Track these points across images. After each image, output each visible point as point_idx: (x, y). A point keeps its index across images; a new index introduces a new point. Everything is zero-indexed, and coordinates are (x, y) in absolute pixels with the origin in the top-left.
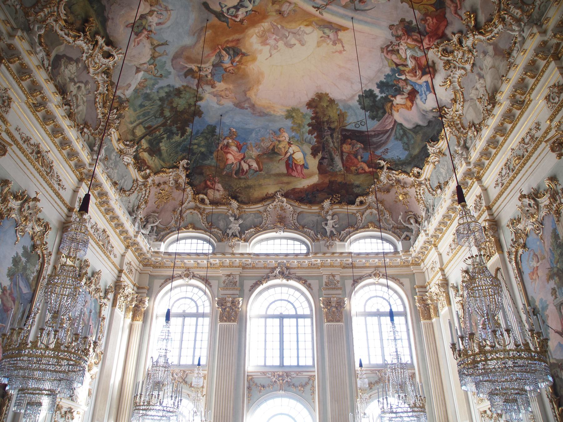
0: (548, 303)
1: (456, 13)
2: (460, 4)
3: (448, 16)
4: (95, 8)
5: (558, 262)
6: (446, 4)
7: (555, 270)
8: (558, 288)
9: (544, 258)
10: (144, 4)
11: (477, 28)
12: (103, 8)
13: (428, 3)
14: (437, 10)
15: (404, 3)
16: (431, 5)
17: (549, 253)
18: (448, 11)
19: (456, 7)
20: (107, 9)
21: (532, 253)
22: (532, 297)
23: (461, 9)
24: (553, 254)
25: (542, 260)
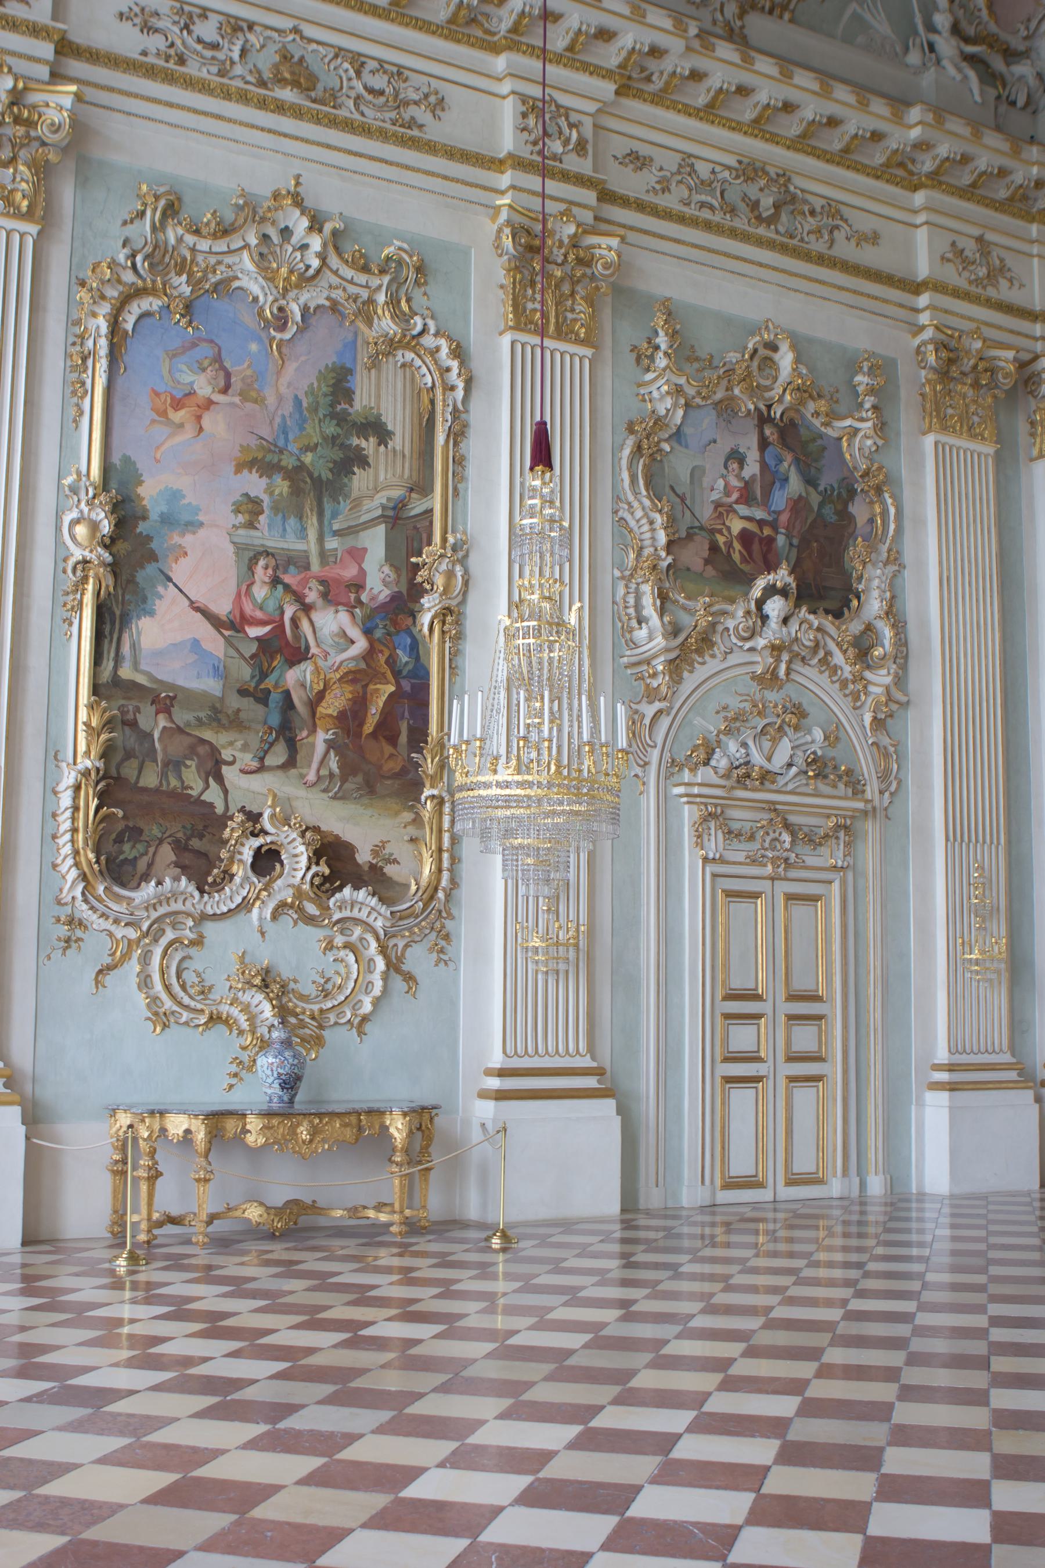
0: (201, 518)
5: (307, 449)
7: (288, 462)
8: (276, 509)
9: (260, 401)
17: (288, 408)
21: (205, 351)
22: (127, 460)
24: (304, 421)
25: (244, 395)
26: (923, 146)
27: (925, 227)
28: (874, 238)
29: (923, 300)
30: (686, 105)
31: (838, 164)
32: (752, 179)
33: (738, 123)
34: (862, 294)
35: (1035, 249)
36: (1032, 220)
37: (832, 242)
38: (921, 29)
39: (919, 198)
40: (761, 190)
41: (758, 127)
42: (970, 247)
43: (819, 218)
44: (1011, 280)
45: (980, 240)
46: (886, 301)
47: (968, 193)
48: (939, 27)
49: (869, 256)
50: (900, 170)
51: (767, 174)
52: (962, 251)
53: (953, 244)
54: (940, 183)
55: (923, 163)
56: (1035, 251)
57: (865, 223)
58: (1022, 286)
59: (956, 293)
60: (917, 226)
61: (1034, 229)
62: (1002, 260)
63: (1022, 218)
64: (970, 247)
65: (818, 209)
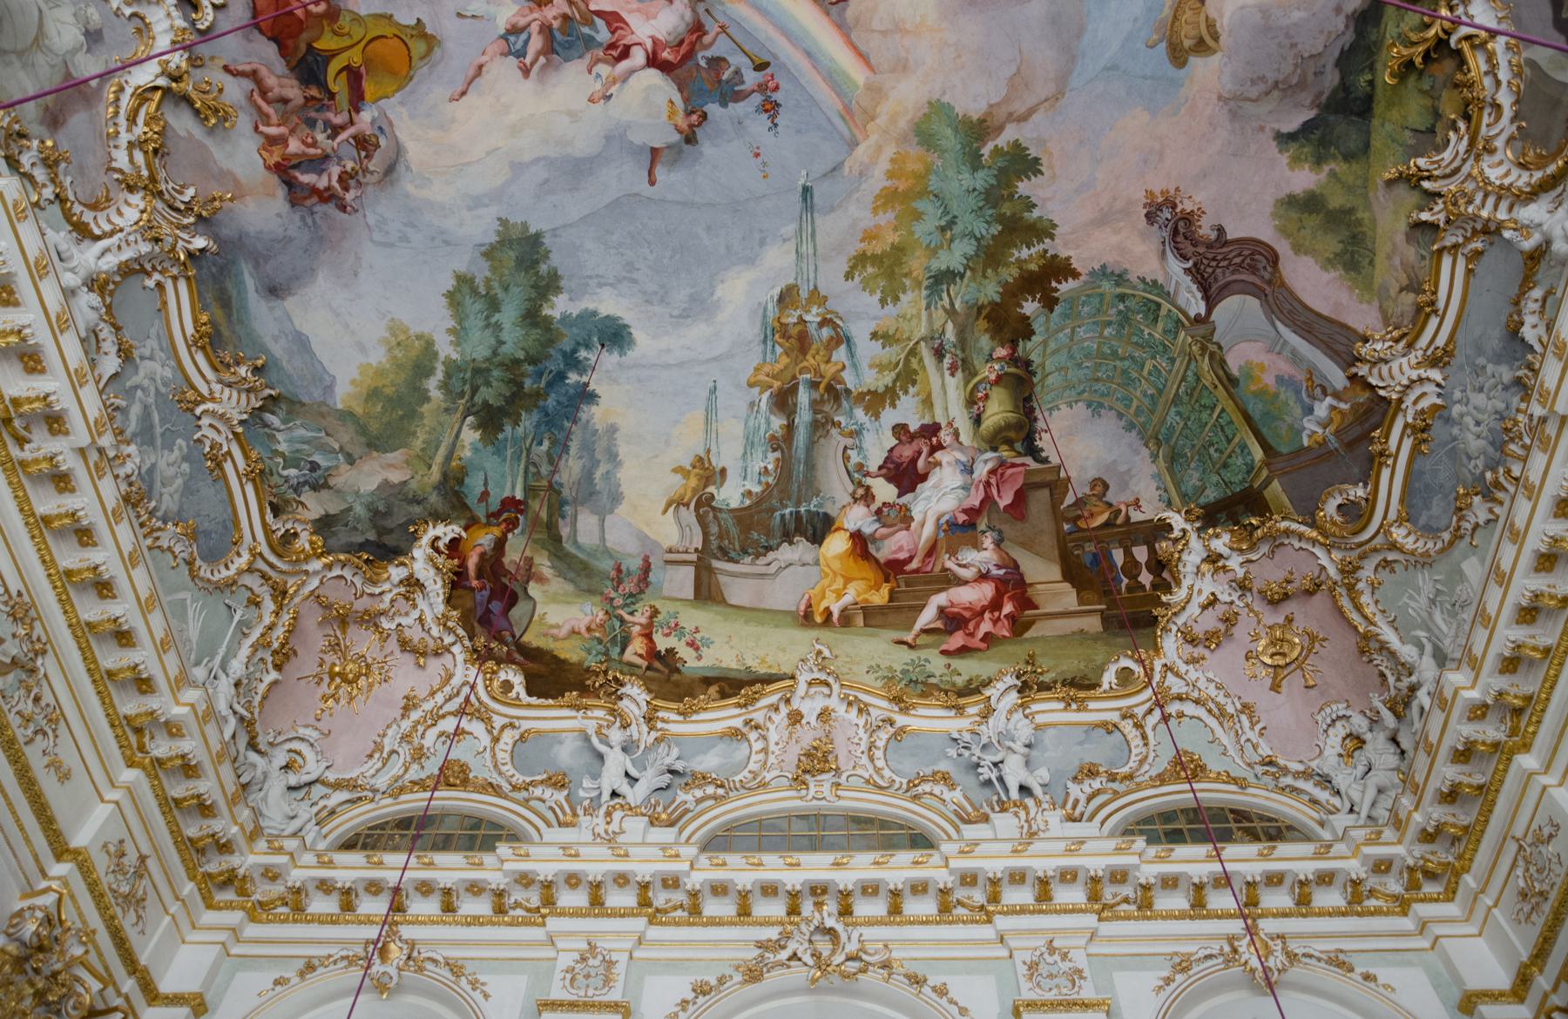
1: (253, 75)
2: (259, 109)
3: (270, 50)
4: (1368, 77)
6: (295, 82)
10: (1221, 17)
11: (172, 94)
12: (1346, 60)
13: (345, 55)
14: (310, 47)
15: (413, 22)
16: (334, 54)
18: (280, 66)
19: (264, 93)
20: (1337, 54)
23: (250, 97)
26: (173, 729)
27: (112, 806)
28: (65, 777)
29: (60, 869)
30: (28, 499)
31: (94, 681)
32: (15, 619)
33: (52, 560)
34: (14, 813)
35: (174, 908)
36: (192, 878)
37: (30, 742)
38: (218, 659)
39: (129, 775)
40: (14, 636)
41: (65, 581)
42: (131, 859)
43: (37, 711)
44: (139, 917)
45: (143, 859)
46: (27, 840)
47: (170, 806)
48: (231, 672)
49: (48, 783)
50: (134, 733)
51: (32, 628)
52: (123, 855)
53: (121, 842)
54: (157, 777)
55: (158, 747)
56: (172, 911)
57: (69, 758)
58: (143, 932)
59: (93, 886)
60: (103, 801)
61: (188, 888)
62: (145, 893)
63: (188, 869)
64: (131, 859)
65: (43, 703)
